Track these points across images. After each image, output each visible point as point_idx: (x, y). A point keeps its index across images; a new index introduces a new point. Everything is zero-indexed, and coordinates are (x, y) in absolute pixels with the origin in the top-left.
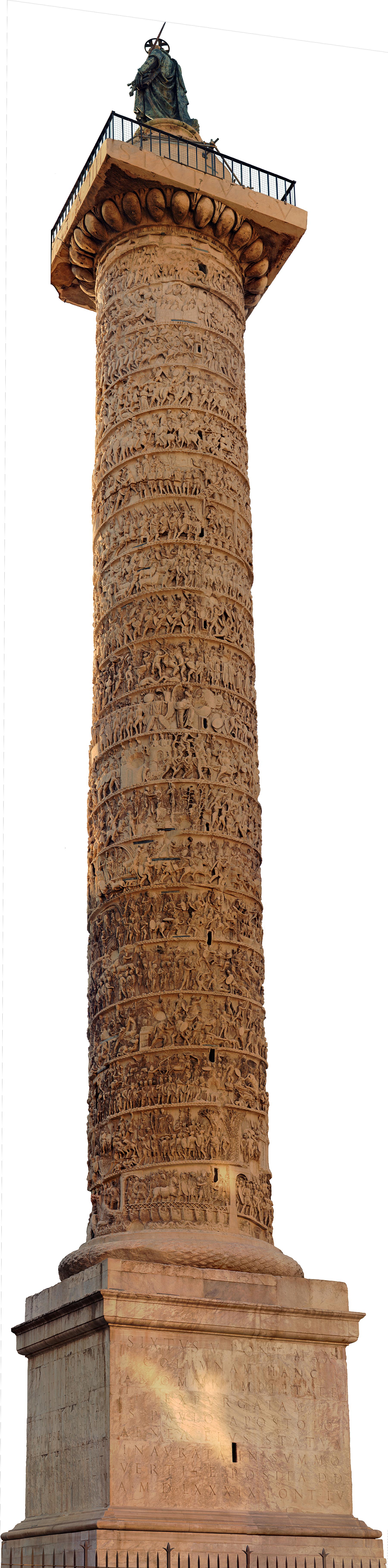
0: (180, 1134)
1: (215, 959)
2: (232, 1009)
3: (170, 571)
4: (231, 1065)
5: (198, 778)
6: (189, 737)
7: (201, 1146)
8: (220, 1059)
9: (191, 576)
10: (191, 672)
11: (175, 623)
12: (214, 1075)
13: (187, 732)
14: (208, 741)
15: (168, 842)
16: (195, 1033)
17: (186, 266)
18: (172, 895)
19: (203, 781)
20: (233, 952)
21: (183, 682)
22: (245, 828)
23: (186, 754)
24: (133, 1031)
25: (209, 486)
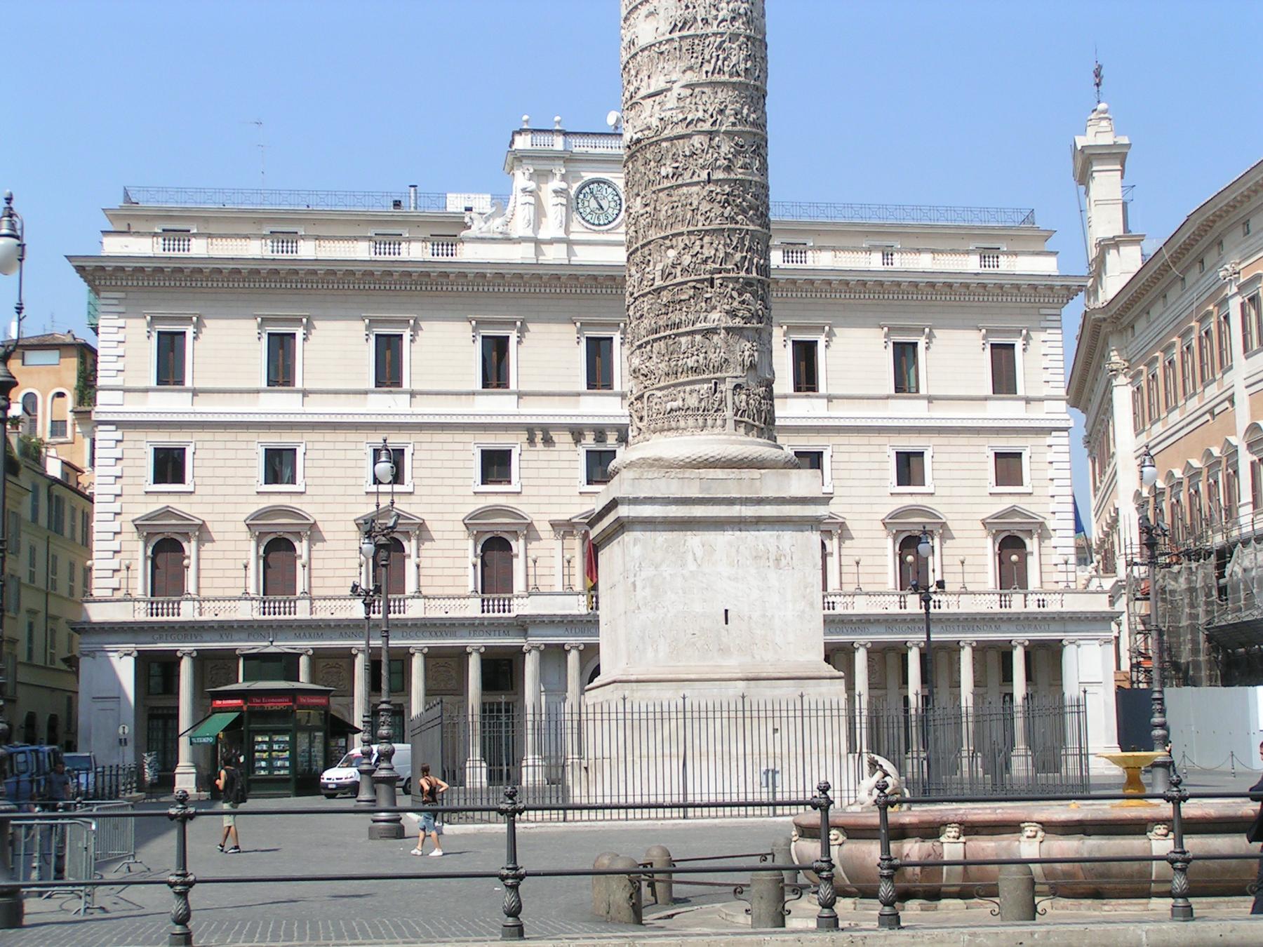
12: (713, 300)
20: (730, 187)
22: (743, 66)
23: (687, 7)
24: (651, 268)
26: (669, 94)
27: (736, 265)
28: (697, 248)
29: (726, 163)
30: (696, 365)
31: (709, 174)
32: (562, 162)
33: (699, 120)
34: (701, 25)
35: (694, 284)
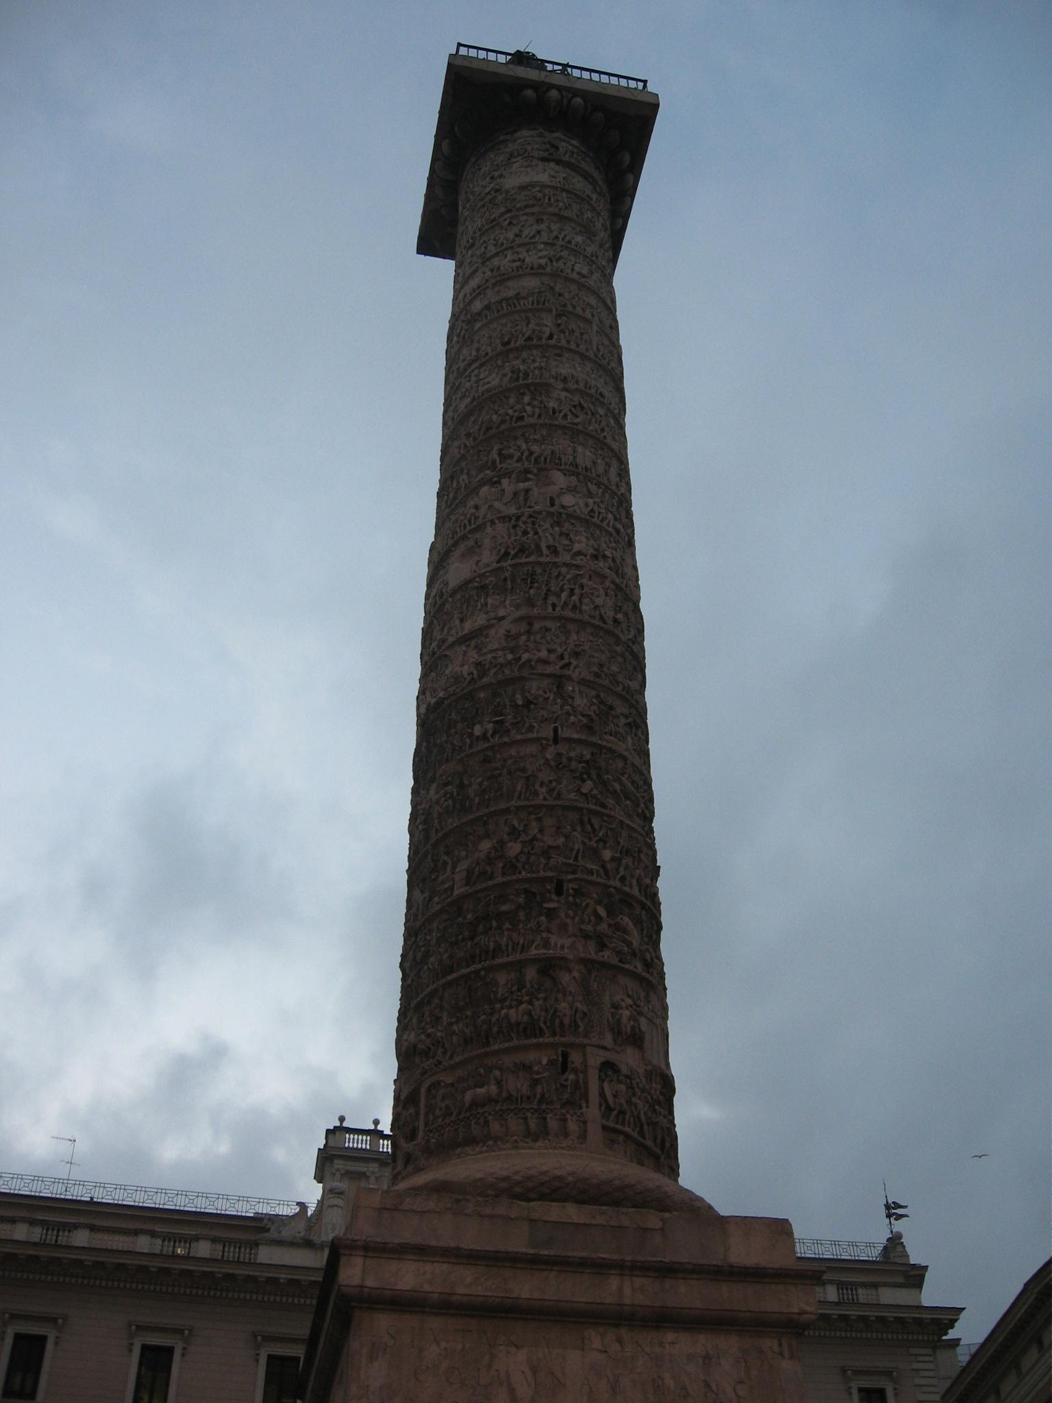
0: (507, 1003)
1: (564, 760)
2: (592, 826)
3: (513, 372)
4: (588, 900)
5: (542, 556)
6: (531, 516)
7: (539, 1017)
8: (571, 891)
9: (536, 372)
10: (535, 455)
11: (517, 414)
13: (527, 511)
14: (555, 518)
15: (502, 632)
16: (532, 858)
17: (536, 147)
18: (505, 691)
19: (548, 559)
20: (592, 754)
21: (526, 466)
23: (525, 533)
25: (561, 298)
26: (492, 632)
27: (603, 867)
28: (534, 831)
29: (585, 720)
30: (525, 1019)
31: (555, 730)
32: (377, 1165)
33: (545, 662)
34: (545, 551)
35: (527, 886)
